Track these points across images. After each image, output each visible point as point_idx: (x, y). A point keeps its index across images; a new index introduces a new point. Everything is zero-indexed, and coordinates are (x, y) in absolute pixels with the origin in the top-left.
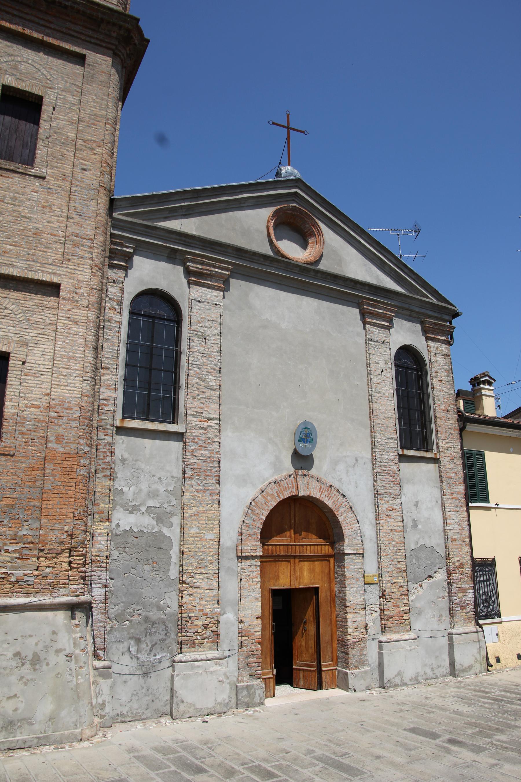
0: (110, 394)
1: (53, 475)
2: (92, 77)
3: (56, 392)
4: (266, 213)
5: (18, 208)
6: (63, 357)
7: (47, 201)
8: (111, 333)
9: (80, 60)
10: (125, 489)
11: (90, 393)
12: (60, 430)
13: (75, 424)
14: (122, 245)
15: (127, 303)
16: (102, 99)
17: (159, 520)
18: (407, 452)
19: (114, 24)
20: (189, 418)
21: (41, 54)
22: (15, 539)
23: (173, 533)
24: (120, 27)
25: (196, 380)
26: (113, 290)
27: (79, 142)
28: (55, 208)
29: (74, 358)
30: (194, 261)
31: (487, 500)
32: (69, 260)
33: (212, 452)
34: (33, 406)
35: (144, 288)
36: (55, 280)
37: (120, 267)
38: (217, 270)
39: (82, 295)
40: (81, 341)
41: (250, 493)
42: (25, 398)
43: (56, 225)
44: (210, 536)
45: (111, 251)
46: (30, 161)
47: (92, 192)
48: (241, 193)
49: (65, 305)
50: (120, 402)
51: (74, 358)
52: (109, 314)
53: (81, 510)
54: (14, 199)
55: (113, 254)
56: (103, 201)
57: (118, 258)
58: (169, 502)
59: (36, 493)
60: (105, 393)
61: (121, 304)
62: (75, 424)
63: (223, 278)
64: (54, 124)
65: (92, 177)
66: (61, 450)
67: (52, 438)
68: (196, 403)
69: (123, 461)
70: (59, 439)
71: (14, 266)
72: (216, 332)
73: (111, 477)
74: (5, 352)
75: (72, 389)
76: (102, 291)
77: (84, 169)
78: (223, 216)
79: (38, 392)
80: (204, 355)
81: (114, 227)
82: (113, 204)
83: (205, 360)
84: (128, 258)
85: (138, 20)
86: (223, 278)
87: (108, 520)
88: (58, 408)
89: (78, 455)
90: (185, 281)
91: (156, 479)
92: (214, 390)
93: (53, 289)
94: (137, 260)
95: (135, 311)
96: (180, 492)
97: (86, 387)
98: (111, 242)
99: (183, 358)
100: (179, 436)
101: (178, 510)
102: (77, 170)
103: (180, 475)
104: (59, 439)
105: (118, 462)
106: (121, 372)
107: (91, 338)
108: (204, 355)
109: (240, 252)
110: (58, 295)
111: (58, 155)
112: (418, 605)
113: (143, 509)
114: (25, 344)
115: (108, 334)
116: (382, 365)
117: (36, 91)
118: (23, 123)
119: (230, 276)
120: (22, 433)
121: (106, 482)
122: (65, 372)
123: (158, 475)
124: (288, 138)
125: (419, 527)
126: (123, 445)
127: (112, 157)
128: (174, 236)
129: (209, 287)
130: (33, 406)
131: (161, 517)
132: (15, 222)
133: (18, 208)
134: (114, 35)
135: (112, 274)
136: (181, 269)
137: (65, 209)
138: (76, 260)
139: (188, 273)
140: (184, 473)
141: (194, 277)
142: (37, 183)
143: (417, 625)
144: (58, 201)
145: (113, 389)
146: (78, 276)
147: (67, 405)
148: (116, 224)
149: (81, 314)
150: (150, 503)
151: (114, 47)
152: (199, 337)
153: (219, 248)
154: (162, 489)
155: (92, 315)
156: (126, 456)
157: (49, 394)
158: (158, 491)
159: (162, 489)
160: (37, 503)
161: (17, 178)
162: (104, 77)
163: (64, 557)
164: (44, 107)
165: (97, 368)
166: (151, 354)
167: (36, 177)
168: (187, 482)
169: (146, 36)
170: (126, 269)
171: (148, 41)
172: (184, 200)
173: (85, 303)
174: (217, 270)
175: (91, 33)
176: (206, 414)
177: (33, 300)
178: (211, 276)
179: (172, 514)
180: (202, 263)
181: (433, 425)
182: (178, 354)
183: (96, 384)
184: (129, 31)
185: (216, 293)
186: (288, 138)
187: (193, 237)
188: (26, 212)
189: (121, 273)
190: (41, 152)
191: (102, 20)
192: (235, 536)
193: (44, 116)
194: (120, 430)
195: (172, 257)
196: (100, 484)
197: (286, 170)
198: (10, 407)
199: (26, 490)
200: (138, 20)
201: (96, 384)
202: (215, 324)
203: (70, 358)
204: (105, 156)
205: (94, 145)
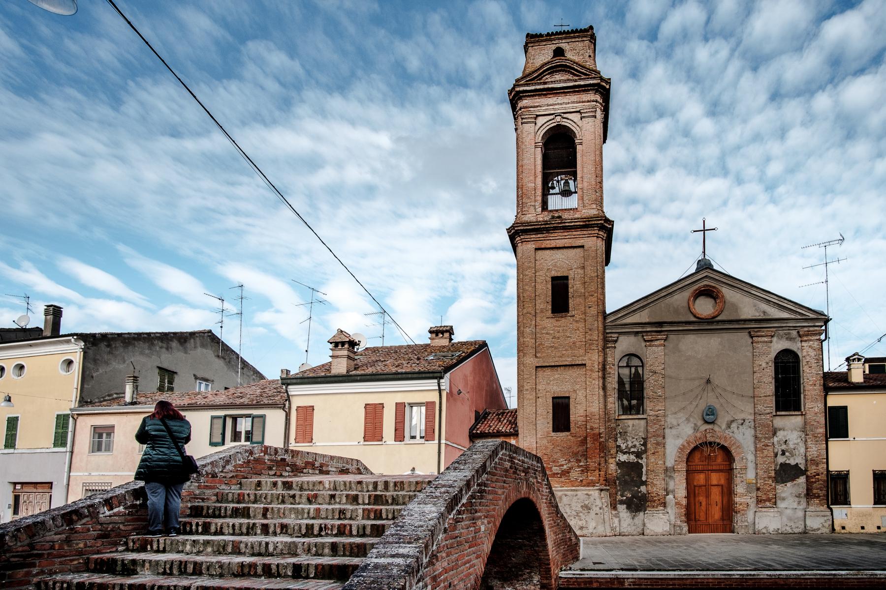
0: (612, 405)
17: (637, 457)
18: (778, 413)
22: (579, 466)
23: (643, 462)
26: (609, 359)
27: (587, 294)
31: (847, 437)
41: (680, 442)
44: (660, 462)
49: (589, 373)
60: (610, 406)
75: (595, 407)
104: (592, 429)
112: (783, 495)
115: (609, 380)
116: (764, 365)
117: (565, 274)
125: (787, 454)
131: (638, 455)
143: (781, 505)
146: (594, 359)
161: (563, 320)
163: (597, 472)
176: (657, 408)
181: (802, 396)
185: (660, 348)
188: (569, 335)
189: (613, 350)
190: (571, 303)
192: (673, 462)
198: (572, 418)
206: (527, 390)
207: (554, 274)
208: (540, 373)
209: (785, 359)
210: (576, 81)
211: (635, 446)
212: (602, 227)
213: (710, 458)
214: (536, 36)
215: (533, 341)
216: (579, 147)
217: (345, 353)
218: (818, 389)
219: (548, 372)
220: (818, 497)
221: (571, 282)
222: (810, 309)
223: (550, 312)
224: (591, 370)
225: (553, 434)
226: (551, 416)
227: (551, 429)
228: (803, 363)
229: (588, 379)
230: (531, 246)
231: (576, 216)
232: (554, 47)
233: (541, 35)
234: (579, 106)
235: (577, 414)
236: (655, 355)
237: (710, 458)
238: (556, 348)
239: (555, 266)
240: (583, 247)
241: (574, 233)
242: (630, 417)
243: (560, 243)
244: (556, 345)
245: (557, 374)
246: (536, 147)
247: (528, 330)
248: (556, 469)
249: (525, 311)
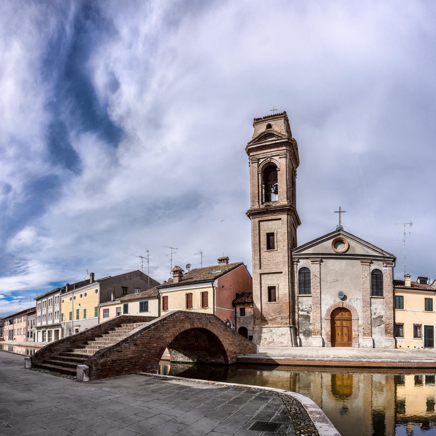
9: (280, 219)
93: (282, 273)
117: (273, 232)
142: (276, 252)
146: (285, 269)
177: (279, 275)
188: (275, 259)
207: (268, 232)
209: (375, 273)
210: (276, 140)
213: (340, 315)
214: (258, 119)
217: (178, 275)
218: (391, 288)
219: (266, 276)
220: (390, 333)
221: (275, 235)
222: (387, 253)
224: (285, 275)
227: (267, 300)
228: (384, 276)
231: (277, 205)
232: (267, 124)
233: (260, 119)
237: (340, 315)
239: (268, 228)
240: (280, 219)
242: (304, 295)
243: (270, 218)
245: (270, 276)
248: (270, 318)
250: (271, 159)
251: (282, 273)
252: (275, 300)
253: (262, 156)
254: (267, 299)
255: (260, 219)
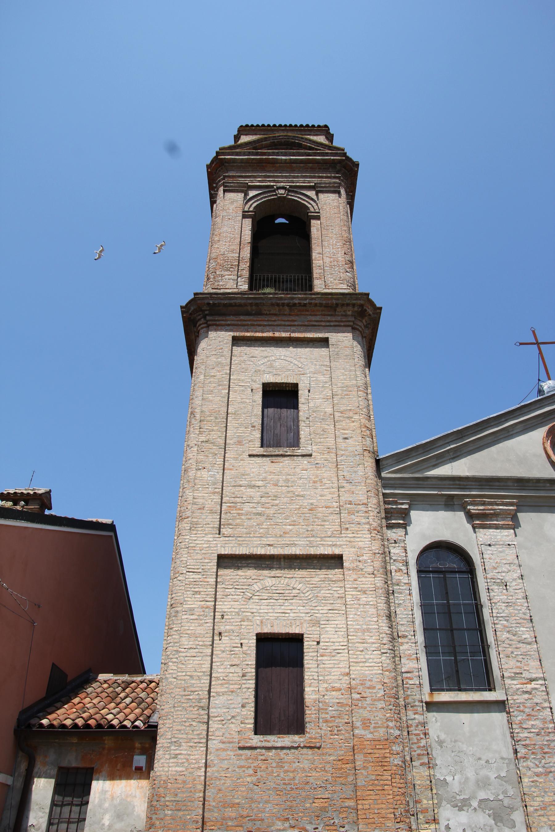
1: (365, 768)
2: (337, 354)
3: (356, 671)
4: (539, 434)
5: (291, 489)
6: (357, 630)
7: (317, 476)
8: (402, 597)
9: (324, 342)
10: (449, 779)
11: (391, 667)
12: (365, 714)
13: (381, 704)
14: (396, 503)
15: (412, 562)
16: (350, 371)
19: (348, 305)
20: (508, 681)
21: (291, 349)
24: (354, 305)
25: (505, 635)
26: (396, 551)
28: (325, 481)
29: (368, 630)
30: (472, 504)
32: (347, 529)
33: (544, 721)
34: (334, 689)
35: (427, 542)
36: (337, 551)
37: (398, 526)
38: (501, 507)
39: (365, 562)
40: (373, 611)
42: (325, 681)
43: (329, 497)
45: (387, 511)
46: (296, 443)
47: (358, 457)
48: (507, 421)
49: (350, 576)
50: (425, 673)
51: (368, 630)
52: (396, 576)
53: (401, 809)
54: (287, 481)
55: (389, 514)
56: (370, 464)
57: (395, 516)
58: (505, 792)
59: (349, 792)
60: (407, 665)
61: (407, 564)
62: (381, 704)
63: (509, 514)
64: (311, 405)
65: (356, 444)
66: (370, 736)
67: (358, 724)
68: (512, 663)
69: (441, 743)
70: (366, 724)
71: (295, 545)
72: (516, 575)
73: (430, 765)
74: (299, 634)
75: (371, 665)
76: (385, 554)
77: (346, 438)
78: (493, 449)
79: (336, 672)
80: (508, 604)
81: (384, 487)
82: (379, 464)
83: (511, 609)
84: (405, 514)
85: (368, 295)
86: (509, 514)
87: (435, 821)
88: (360, 689)
89: (388, 741)
90: (469, 527)
91: (483, 762)
92: (529, 644)
93: (335, 561)
94: (414, 514)
95: (422, 569)
96: (515, 779)
97: (386, 660)
98: (385, 503)
99: (486, 612)
100: (500, 706)
101: (518, 803)
102: (340, 440)
103: (512, 756)
104: (366, 724)
105: (435, 745)
106: (420, 638)
107: (382, 606)
108: (508, 604)
109: (521, 483)
110: (342, 567)
111: (319, 431)
113: (475, 804)
114: (317, 623)
115: (399, 598)
117: (291, 380)
118: (284, 411)
119: (517, 511)
120: (326, 721)
121: (425, 772)
122: (361, 647)
123: (484, 758)
124: (540, 353)
126: (437, 722)
127: (369, 420)
128: (447, 482)
129: (497, 527)
130: (334, 689)
132: (291, 502)
133: (291, 489)
134: (350, 313)
135: (392, 534)
136: (462, 514)
137: (335, 479)
138: (354, 527)
139: (470, 517)
140: (516, 752)
141: (478, 521)
142: (305, 461)
144: (328, 473)
145: (415, 660)
146: (358, 543)
147: (368, 684)
148: (386, 483)
149: (368, 582)
150: (482, 795)
151: (351, 324)
152: (498, 584)
153: (497, 484)
154: (493, 776)
155: (379, 581)
156: (443, 736)
157: (348, 674)
158: (488, 778)
159: (493, 776)
160: (351, 803)
162: (348, 352)
164: (300, 392)
165: (394, 638)
166: (449, 613)
167: (303, 456)
168: (522, 764)
169: (378, 305)
170: (404, 526)
171: (380, 309)
172: (449, 444)
173: (370, 569)
174: (501, 507)
175: (329, 318)
176: (526, 675)
178: (496, 515)
179: (512, 809)
180: (484, 504)
182: (478, 608)
183: (396, 656)
184: (362, 306)
185: (505, 532)
186: (540, 353)
187: (467, 479)
188: (299, 491)
190: (304, 433)
191: (337, 305)
193: (301, 400)
194: (431, 706)
195: (450, 504)
196: (419, 774)
197: (547, 385)
198: (310, 694)
199: (338, 788)
200: (368, 295)
201: (396, 656)
202: (513, 567)
203: (364, 631)
204: (364, 421)
205: (351, 414)
206: (191, 611)
208: (227, 574)
211: (483, 783)
212: (361, 313)
215: (217, 498)
216: (313, 222)
223: (258, 443)
225: (257, 740)
226: (252, 684)
229: (351, 593)
230: (226, 336)
234: (313, 182)
235: (321, 679)
236: (492, 550)
238: (269, 518)
239: (271, 366)
241: (309, 318)
244: (271, 511)
246: (244, 217)
247: (204, 474)
249: (203, 438)
250: (289, 191)
251: (335, 561)
252: (298, 726)
253: (259, 181)
254: (249, 712)
255: (237, 334)
